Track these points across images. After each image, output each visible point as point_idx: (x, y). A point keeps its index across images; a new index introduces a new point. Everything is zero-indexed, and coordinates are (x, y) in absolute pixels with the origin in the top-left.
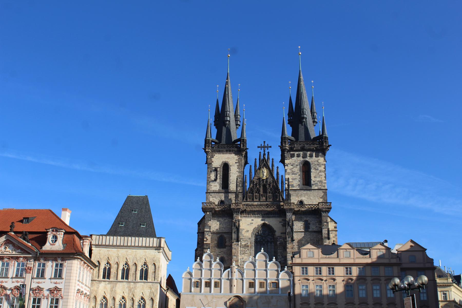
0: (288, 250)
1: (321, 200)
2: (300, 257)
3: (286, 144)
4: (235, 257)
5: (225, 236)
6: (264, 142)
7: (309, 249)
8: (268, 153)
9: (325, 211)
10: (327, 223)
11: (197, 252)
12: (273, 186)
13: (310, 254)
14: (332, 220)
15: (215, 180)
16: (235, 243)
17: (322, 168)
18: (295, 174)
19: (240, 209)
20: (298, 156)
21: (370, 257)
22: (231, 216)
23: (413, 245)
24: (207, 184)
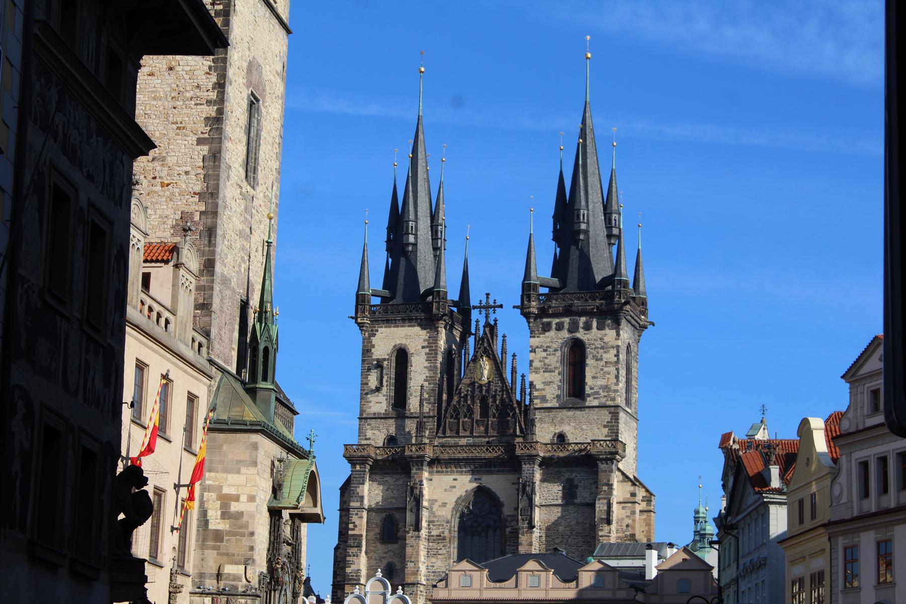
0: (520, 548)
1: (601, 433)
2: (447, 586)
3: (529, 301)
4: (412, 565)
5: (397, 516)
6: (488, 295)
7: (464, 571)
8: (495, 321)
9: (606, 460)
10: (610, 486)
11: (338, 554)
12: (502, 400)
13: (465, 581)
14: (627, 477)
15: (378, 389)
16: (412, 533)
17: (610, 356)
18: (551, 371)
19: (423, 456)
20: (559, 327)
21: (577, 586)
22: (407, 472)
23: (687, 557)
24: (362, 399)
